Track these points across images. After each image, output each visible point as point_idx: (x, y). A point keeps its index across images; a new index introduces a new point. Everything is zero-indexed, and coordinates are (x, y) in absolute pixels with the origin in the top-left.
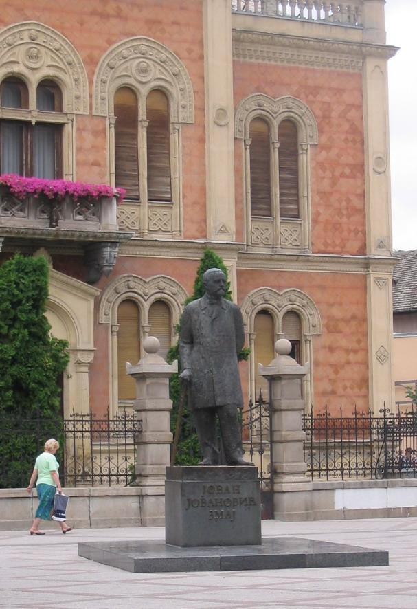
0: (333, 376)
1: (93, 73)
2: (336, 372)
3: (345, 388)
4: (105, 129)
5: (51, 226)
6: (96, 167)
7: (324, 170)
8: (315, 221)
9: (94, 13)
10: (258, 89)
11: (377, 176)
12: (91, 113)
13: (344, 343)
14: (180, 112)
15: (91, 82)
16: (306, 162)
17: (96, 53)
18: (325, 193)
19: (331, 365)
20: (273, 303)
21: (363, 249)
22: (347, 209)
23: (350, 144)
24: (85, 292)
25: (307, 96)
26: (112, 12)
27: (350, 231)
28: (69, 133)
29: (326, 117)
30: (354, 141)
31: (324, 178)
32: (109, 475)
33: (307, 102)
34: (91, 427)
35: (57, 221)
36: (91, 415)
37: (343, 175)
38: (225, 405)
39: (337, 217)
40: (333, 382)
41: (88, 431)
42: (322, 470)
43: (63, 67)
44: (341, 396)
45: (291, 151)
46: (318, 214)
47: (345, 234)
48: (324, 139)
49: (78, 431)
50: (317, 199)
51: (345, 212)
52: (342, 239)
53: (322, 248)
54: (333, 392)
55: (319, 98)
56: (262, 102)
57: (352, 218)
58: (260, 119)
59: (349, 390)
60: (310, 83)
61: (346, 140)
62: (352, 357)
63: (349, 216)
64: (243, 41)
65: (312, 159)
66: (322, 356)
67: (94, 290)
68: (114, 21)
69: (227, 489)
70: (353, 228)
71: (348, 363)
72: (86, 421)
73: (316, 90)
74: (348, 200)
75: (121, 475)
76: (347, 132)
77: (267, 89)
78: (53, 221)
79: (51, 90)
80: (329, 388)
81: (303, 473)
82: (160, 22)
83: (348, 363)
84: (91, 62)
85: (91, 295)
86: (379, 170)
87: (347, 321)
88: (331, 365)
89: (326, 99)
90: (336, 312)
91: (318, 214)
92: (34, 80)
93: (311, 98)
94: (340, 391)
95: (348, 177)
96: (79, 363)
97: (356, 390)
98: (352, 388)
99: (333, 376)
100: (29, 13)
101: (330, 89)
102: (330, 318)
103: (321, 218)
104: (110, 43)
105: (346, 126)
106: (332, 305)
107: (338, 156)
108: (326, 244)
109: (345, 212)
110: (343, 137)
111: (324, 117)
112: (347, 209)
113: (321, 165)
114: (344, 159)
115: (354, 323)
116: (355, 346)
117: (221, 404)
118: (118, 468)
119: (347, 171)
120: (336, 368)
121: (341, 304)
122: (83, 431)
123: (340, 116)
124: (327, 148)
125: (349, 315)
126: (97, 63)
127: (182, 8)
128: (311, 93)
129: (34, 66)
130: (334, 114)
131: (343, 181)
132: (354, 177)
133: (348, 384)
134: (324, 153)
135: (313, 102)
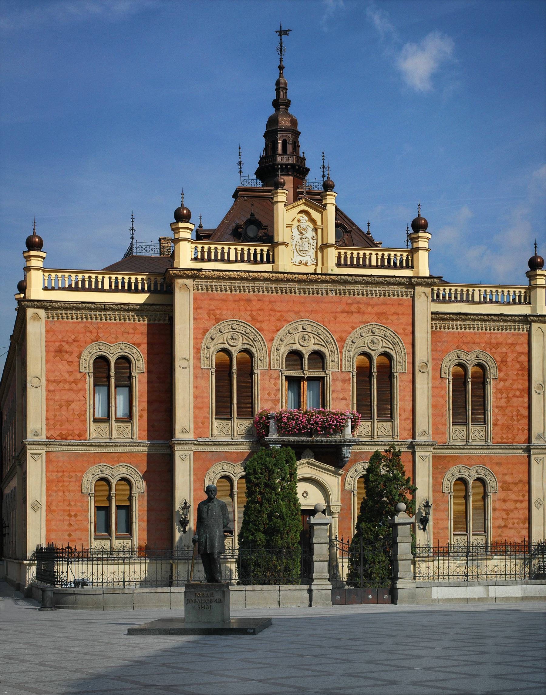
0: (505, 516)
1: (343, 346)
2: (508, 514)
3: (514, 524)
4: (350, 378)
6: (344, 401)
7: (501, 393)
8: (495, 425)
9: (343, 312)
10: (458, 347)
12: (342, 371)
13: (513, 497)
14: (400, 367)
15: (341, 352)
16: (491, 388)
17: (344, 335)
18: (502, 407)
19: (504, 510)
20: (474, 474)
21: (529, 440)
22: (517, 416)
23: (520, 377)
26: (354, 310)
27: (519, 430)
28: (329, 381)
29: (504, 361)
30: (523, 375)
31: (501, 398)
33: (491, 353)
37: (514, 396)
39: (510, 422)
40: (505, 520)
43: (324, 344)
44: (511, 528)
45: (481, 381)
46: (497, 420)
47: (515, 431)
48: (502, 375)
50: (496, 411)
51: (515, 418)
52: (513, 435)
53: (500, 440)
54: (505, 526)
55: (499, 350)
56: (460, 355)
57: (520, 422)
58: (459, 365)
59: (516, 524)
60: (493, 341)
61: (517, 374)
62: (518, 505)
63: (518, 420)
64: (447, 319)
65: (493, 387)
68: (356, 315)
70: (520, 428)
71: (516, 508)
73: (498, 345)
74: (518, 411)
76: (518, 370)
77: (464, 347)
79: (318, 357)
80: (503, 524)
82: (385, 314)
83: (516, 508)
84: (342, 340)
86: (538, 391)
87: (516, 484)
88: (504, 510)
89: (504, 350)
90: (508, 478)
91: (497, 420)
92: (306, 353)
93: (494, 350)
94: (510, 525)
95: (517, 397)
97: (521, 525)
98: (518, 524)
100: (302, 315)
101: (507, 344)
103: (499, 423)
104: (353, 328)
105: (518, 366)
106: (506, 474)
108: (502, 438)
109: (515, 418)
110: (515, 373)
111: (502, 361)
113: (500, 391)
114: (515, 387)
115: (520, 485)
116: (521, 498)
119: (518, 393)
120: (507, 512)
123: (513, 360)
124: (503, 380)
125: (517, 480)
126: (345, 341)
127: (399, 304)
129: (305, 345)
130: (509, 359)
131: (515, 399)
132: (523, 397)
133: (516, 521)
134: (502, 384)
135: (496, 353)
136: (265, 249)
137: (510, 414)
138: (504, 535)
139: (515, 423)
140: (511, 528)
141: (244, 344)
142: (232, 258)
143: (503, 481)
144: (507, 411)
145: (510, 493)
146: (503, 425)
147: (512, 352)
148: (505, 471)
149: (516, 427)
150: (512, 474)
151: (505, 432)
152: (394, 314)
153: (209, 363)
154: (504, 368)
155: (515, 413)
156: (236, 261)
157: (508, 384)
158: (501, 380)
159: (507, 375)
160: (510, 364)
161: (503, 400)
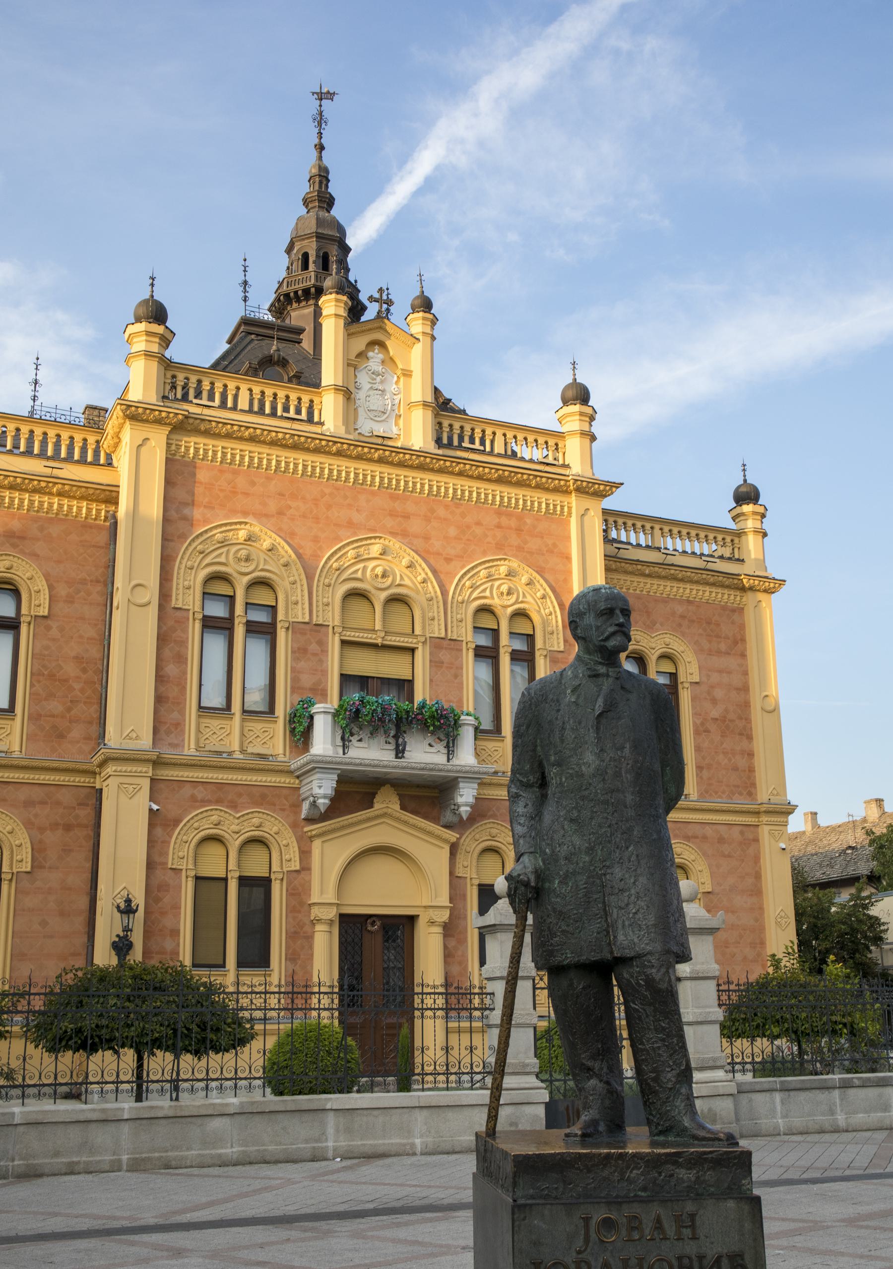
5: (397, 757)
24: (438, 837)
32: (447, 1073)
34: (447, 1002)
35: (403, 751)
36: (447, 985)
38: (639, 956)
41: (442, 1009)
42: (746, 1063)
49: (427, 1009)
67: (452, 836)
69: (658, 1225)
72: (439, 994)
75: (464, 1073)
78: (400, 752)
81: (722, 1067)
85: (446, 841)
96: (432, 923)
117: (628, 953)
118: (459, 1063)
122: (434, 1009)
136: (305, 399)
141: (262, 570)
142: (243, 404)
153: (188, 596)
156: (250, 411)
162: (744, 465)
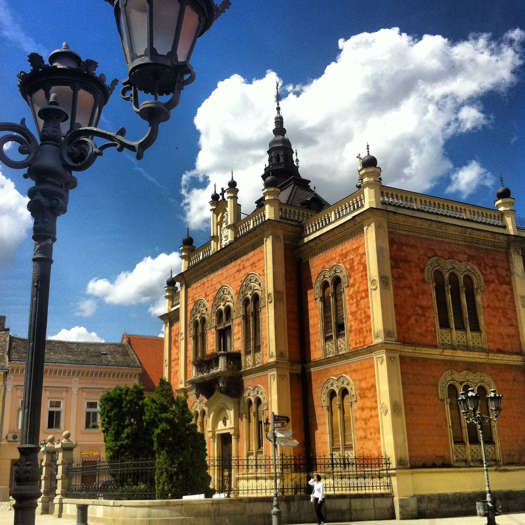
0: (364, 427)
2: (366, 424)
3: (371, 434)
11: (373, 292)
25: (343, 260)
31: (352, 304)
40: (365, 430)
44: (370, 439)
46: (351, 326)
47: (365, 333)
51: (364, 320)
53: (355, 346)
54: (365, 437)
55: (348, 258)
59: (373, 435)
61: (362, 275)
66: (358, 414)
71: (372, 416)
73: (347, 254)
80: (363, 435)
89: (352, 257)
94: (369, 436)
99: (364, 427)
101: (352, 250)
102: (361, 389)
103: (353, 328)
107: (359, 287)
110: (360, 275)
111: (351, 268)
112: (365, 318)
121: (365, 379)
123: (358, 264)
128: (344, 257)
133: (372, 431)
134: (352, 289)
137: (360, 318)
138: (365, 447)
139: (364, 325)
140: (370, 439)
143: (360, 388)
144: (358, 315)
145: (365, 400)
146: (356, 329)
147: (357, 256)
148: (361, 378)
149: (364, 329)
150: (365, 379)
151: (358, 336)
152: (259, 260)
154: (352, 274)
155: (363, 315)
157: (356, 288)
158: (351, 286)
159: (355, 279)
160: (356, 268)
161: (354, 305)
162: (368, 146)
